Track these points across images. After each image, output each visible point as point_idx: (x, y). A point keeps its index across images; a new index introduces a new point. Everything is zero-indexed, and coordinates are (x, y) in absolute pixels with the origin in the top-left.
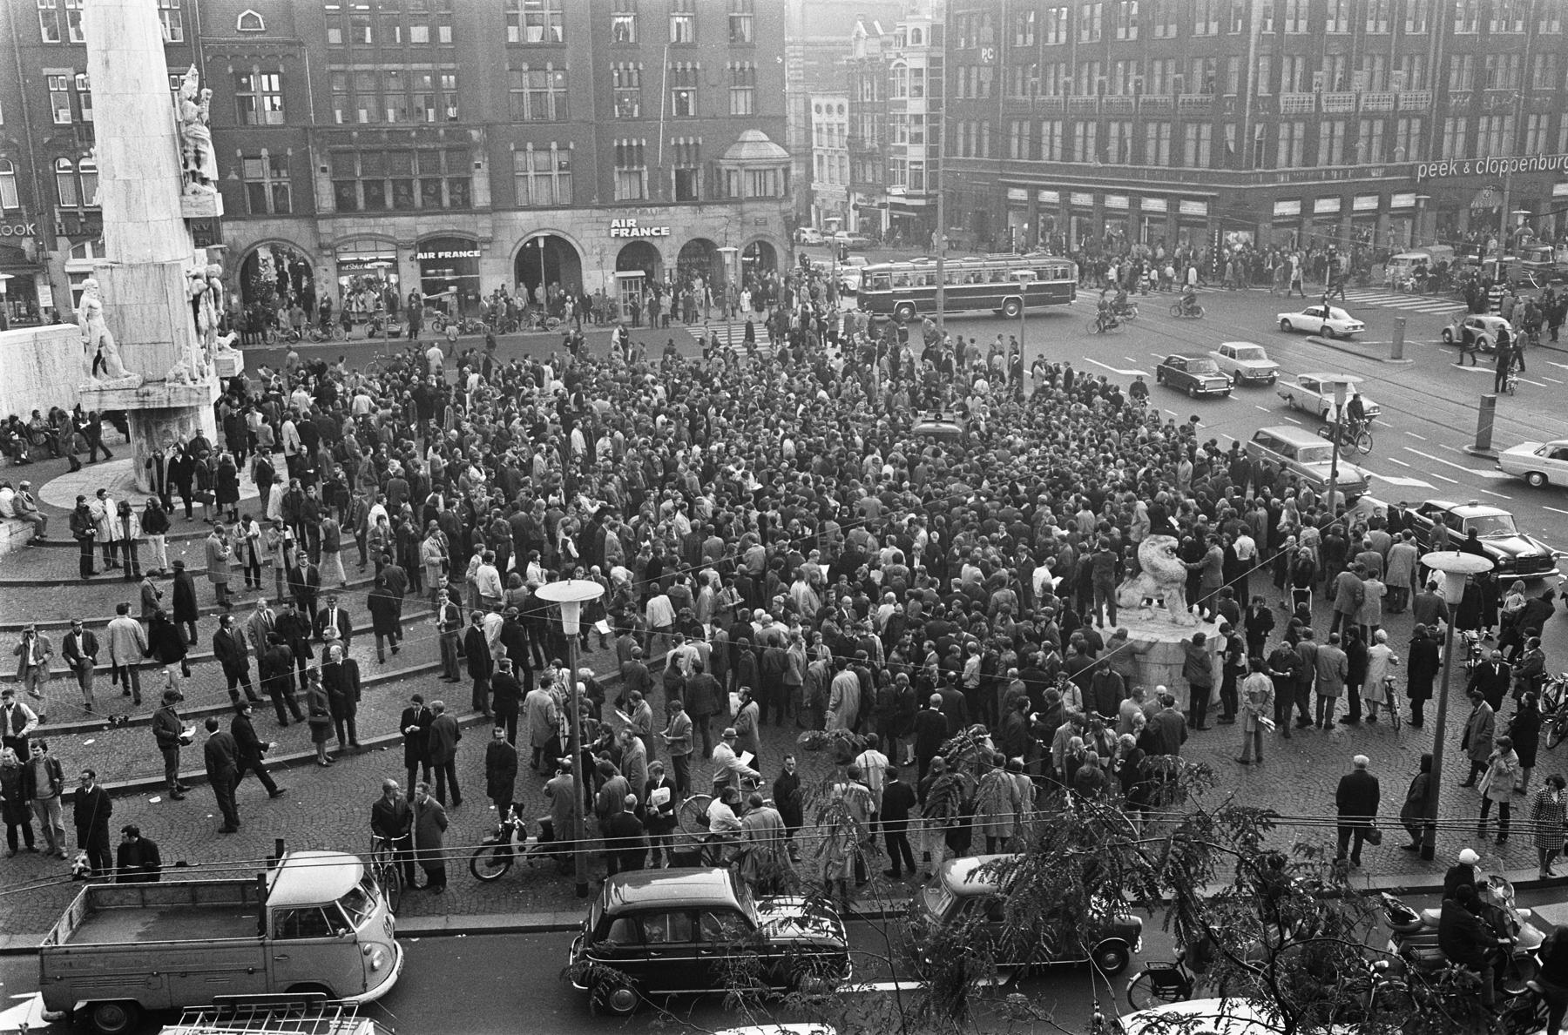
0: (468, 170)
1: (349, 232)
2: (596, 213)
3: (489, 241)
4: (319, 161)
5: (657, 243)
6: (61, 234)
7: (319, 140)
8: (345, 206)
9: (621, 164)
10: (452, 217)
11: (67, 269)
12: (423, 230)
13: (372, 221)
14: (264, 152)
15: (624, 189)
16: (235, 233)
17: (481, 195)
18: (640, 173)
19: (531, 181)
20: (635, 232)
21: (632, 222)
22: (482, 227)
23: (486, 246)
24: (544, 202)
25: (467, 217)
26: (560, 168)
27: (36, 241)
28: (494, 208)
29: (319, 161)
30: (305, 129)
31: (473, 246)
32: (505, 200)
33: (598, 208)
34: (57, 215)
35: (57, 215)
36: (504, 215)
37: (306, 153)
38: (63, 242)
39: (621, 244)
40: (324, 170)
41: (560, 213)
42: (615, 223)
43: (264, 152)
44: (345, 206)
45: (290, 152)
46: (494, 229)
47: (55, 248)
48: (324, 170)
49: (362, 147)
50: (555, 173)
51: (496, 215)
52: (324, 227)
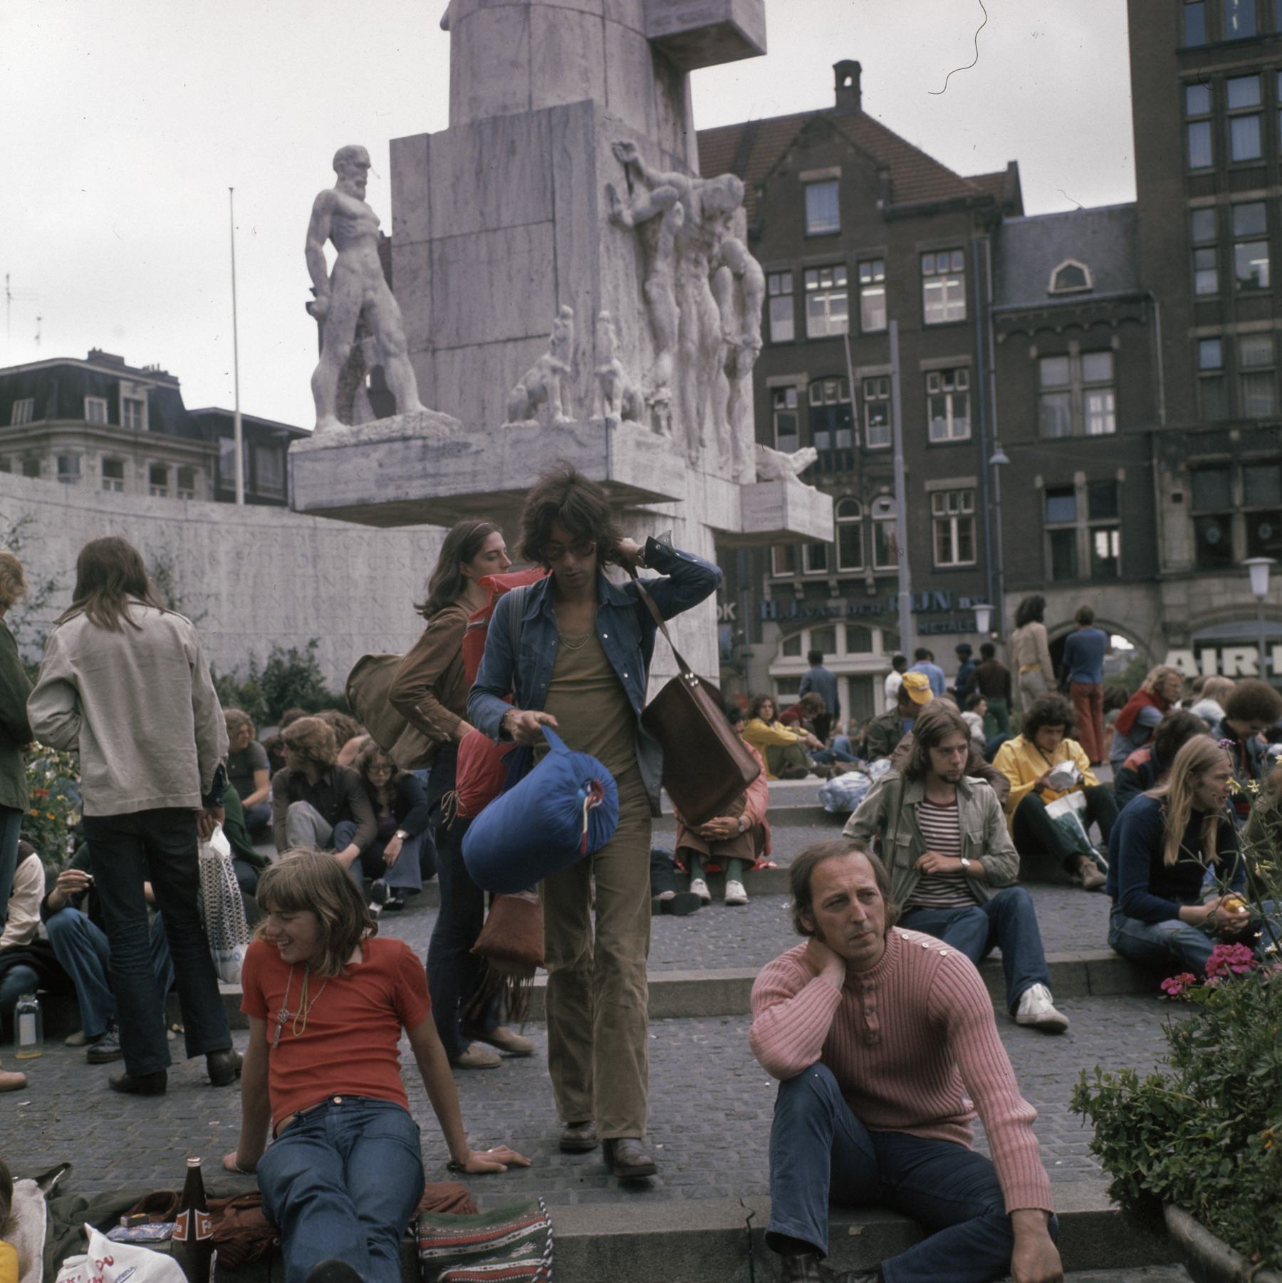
1: (1219, 601)
4: (1169, 484)
6: (769, 618)
7: (1172, 450)
11: (774, 671)
14: (1080, 478)
27: (735, 629)
29: (1169, 484)
30: (1149, 435)
34: (767, 590)
35: (767, 590)
37: (1150, 470)
38: (771, 631)
40: (1177, 498)
43: (1080, 478)
45: (1121, 475)
47: (758, 639)
48: (1177, 498)
49: (1249, 454)
52: (1174, 596)
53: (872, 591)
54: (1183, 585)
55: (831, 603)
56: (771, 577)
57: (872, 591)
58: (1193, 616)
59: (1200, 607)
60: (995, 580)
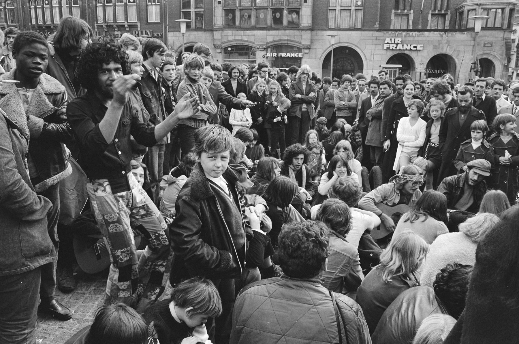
0: (300, 5)
1: (230, 38)
2: (376, 34)
3: (309, 48)
5: (413, 55)
8: (230, 24)
9: (397, 8)
10: (287, 32)
12: (270, 39)
13: (242, 32)
15: (396, 22)
16: (174, 38)
17: (306, 19)
18: (407, 15)
19: (338, 12)
20: (400, 47)
21: (399, 40)
22: (305, 38)
23: (307, 51)
24: (345, 25)
25: (296, 32)
26: (357, 5)
28: (312, 29)
31: (299, 50)
32: (319, 23)
33: (378, 31)
34: (96, 27)
36: (320, 33)
39: (390, 54)
41: (354, 33)
42: (388, 40)
44: (230, 24)
46: (312, 41)
50: (353, 8)
51: (314, 32)
52: (217, 35)
53: (128, 29)
54: (220, 32)
55: (116, 33)
56: (97, 23)
57: (128, 29)
58: (223, 43)
59: (224, 40)
60: (165, 28)
